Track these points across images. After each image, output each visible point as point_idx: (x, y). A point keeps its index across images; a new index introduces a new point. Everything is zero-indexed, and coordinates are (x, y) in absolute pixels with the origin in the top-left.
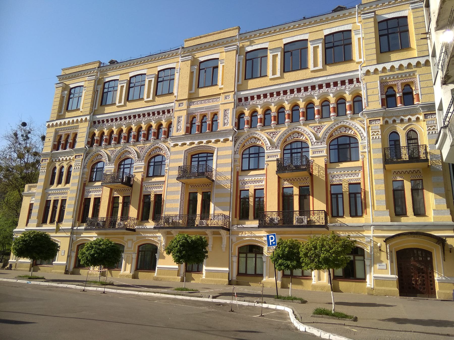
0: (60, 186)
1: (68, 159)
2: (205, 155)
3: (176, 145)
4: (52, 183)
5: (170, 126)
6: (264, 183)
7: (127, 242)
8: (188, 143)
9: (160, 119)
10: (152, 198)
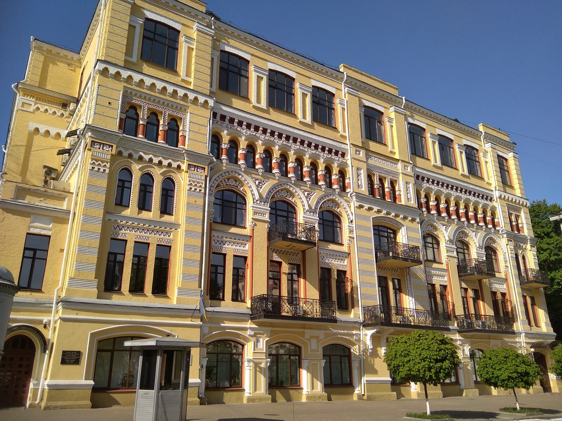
0: (145, 215)
1: (165, 163)
2: (386, 230)
3: (361, 207)
4: (122, 202)
5: (342, 174)
6: (446, 279)
7: (309, 340)
8: (376, 208)
9: (318, 156)
10: (335, 275)
